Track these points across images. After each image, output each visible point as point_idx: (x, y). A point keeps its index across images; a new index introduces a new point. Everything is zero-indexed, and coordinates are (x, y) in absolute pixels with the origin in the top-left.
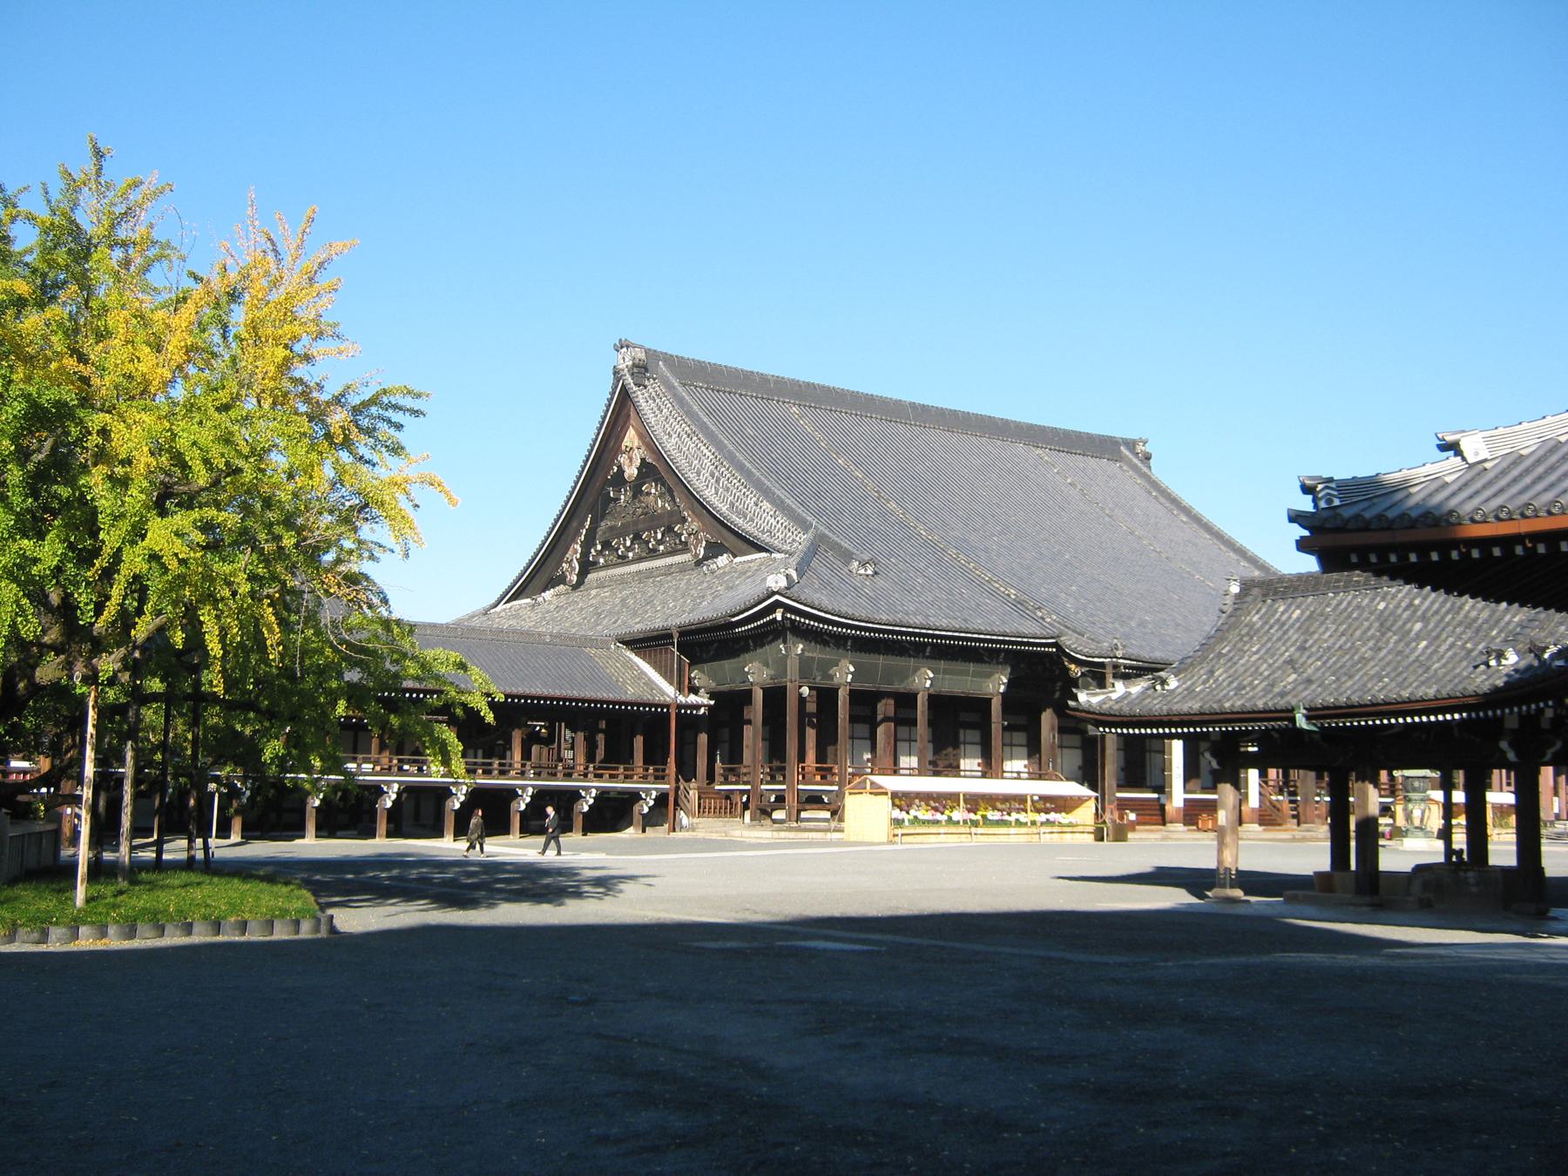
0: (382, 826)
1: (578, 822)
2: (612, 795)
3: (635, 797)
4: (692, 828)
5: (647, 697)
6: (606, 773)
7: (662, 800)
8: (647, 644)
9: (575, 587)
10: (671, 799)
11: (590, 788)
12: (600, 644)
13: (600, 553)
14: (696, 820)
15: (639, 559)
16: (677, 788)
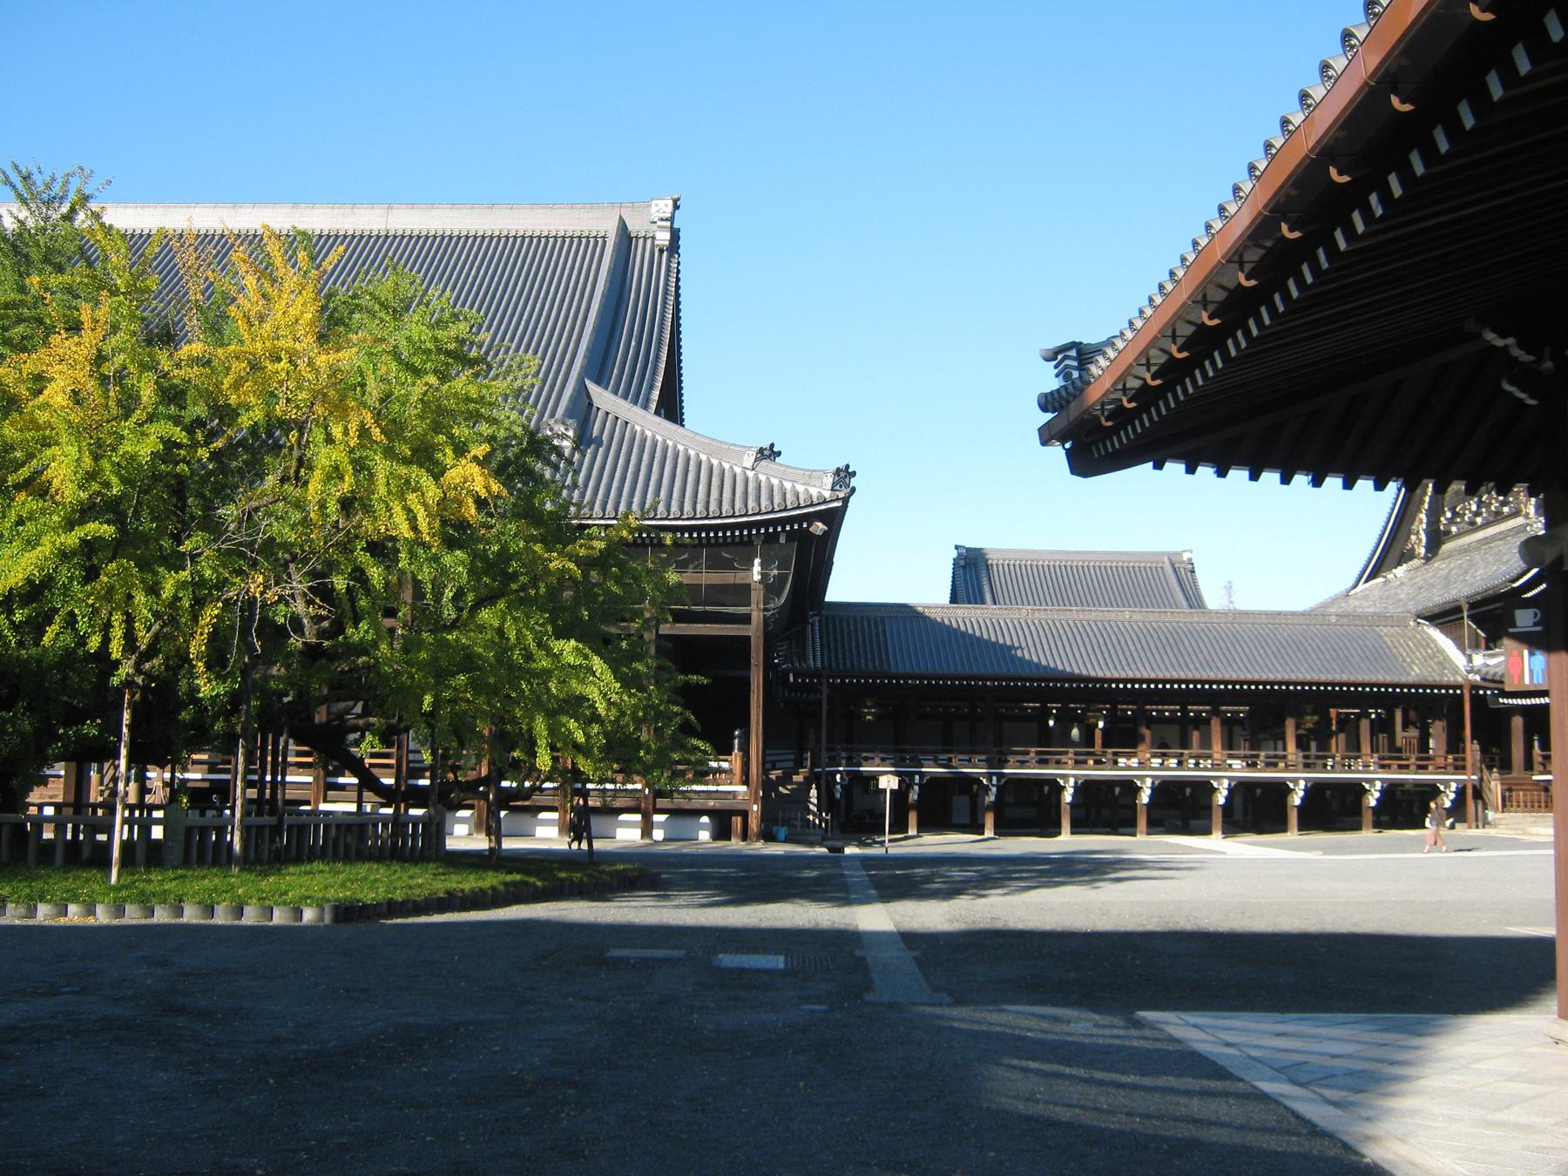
0: (1142, 822)
1: (1368, 817)
2: (1407, 787)
3: (1432, 791)
4: (1495, 826)
5: (1434, 678)
6: (1395, 763)
7: (1461, 793)
8: (1445, 617)
9: (1427, 559)
10: (1469, 792)
11: (1374, 779)
12: (1399, 622)
13: (1451, 521)
14: (1500, 815)
15: (1486, 525)
16: (1481, 780)
